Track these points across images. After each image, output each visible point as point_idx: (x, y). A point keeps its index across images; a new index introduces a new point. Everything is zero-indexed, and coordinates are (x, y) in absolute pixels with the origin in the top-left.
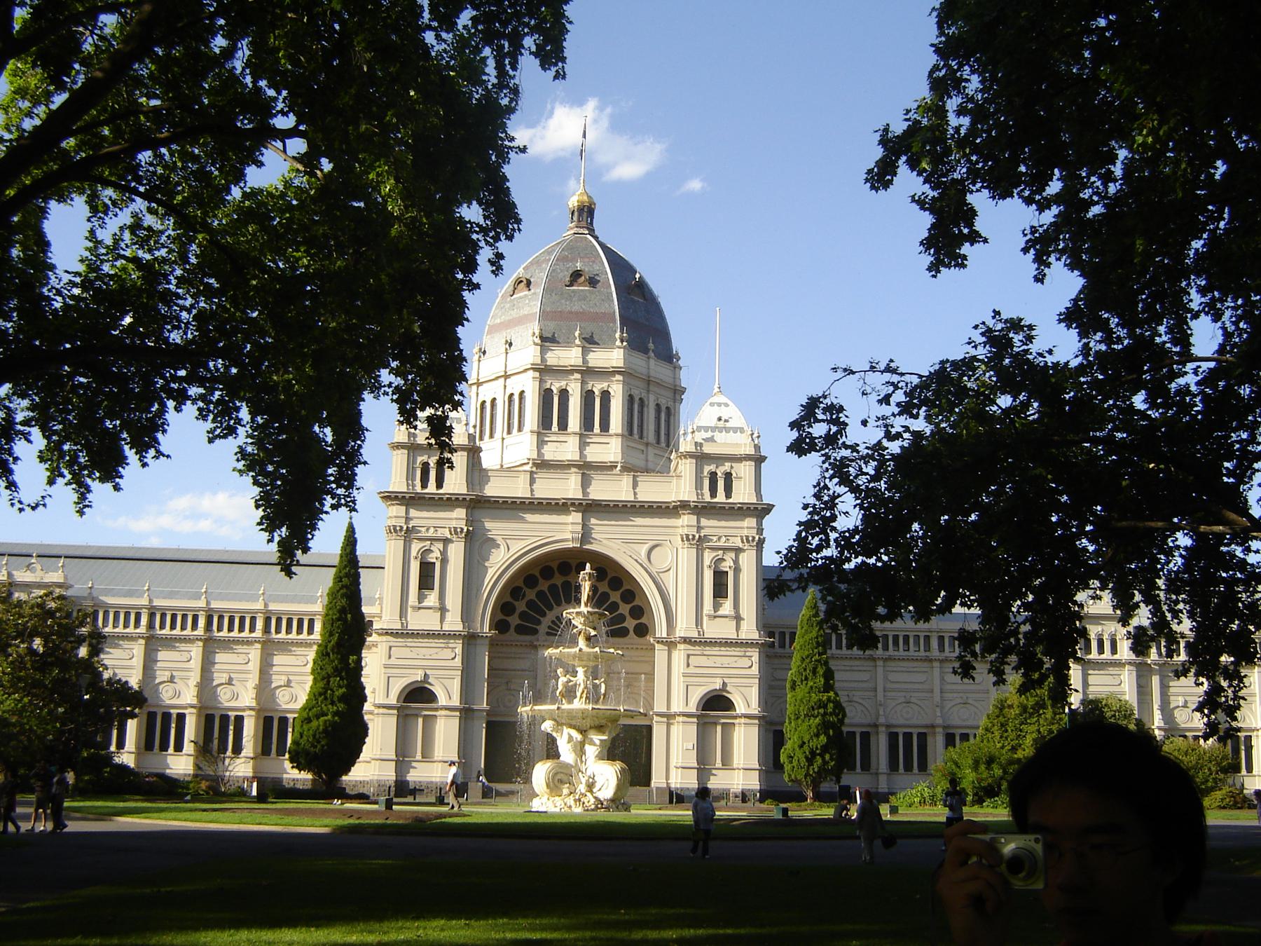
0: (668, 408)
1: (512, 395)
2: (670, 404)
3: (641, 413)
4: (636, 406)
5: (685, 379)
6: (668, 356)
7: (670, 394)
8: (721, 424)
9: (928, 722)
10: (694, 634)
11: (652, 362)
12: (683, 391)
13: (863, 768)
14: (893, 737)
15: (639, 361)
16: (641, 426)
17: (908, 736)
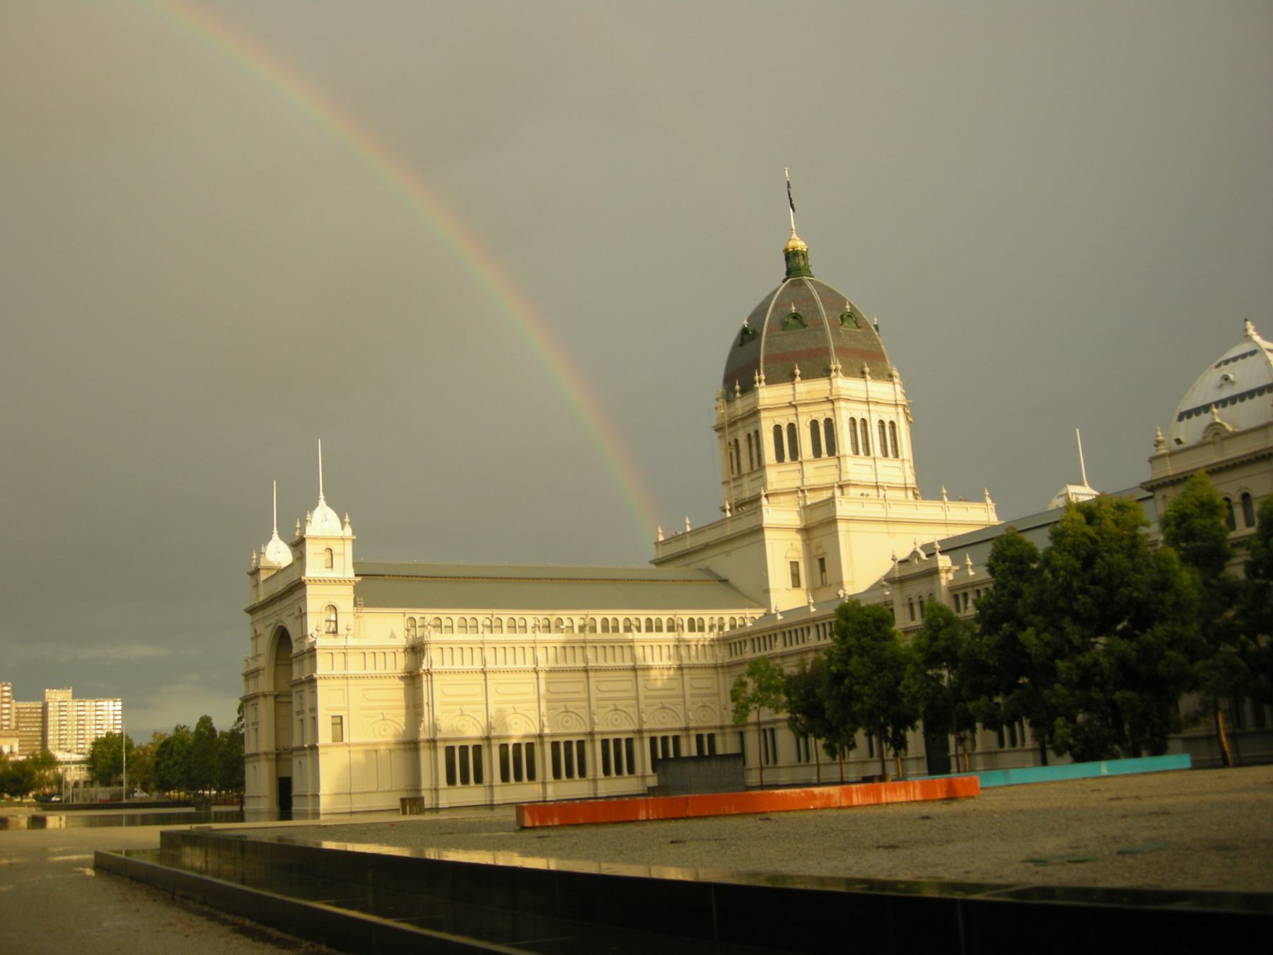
1: (749, 435)
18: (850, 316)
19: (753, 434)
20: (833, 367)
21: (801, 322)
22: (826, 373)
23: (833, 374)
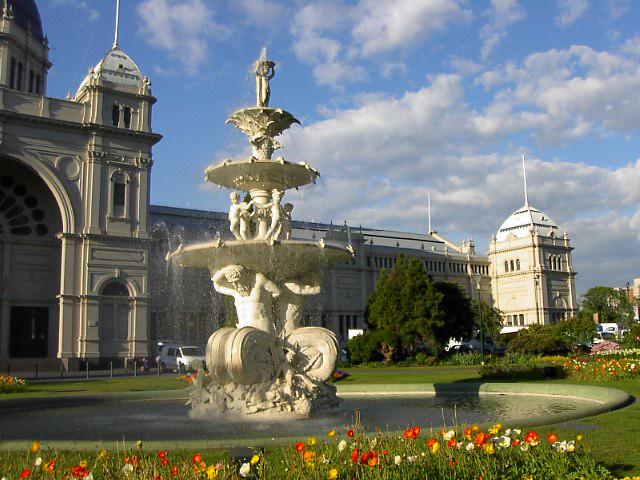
0: (38, 76)
2: (40, 73)
3: (20, 73)
4: (16, 68)
5: (51, 57)
6: (40, 39)
8: (121, 71)
10: (99, 233)
11: (30, 39)
12: (49, 65)
15: (20, 36)
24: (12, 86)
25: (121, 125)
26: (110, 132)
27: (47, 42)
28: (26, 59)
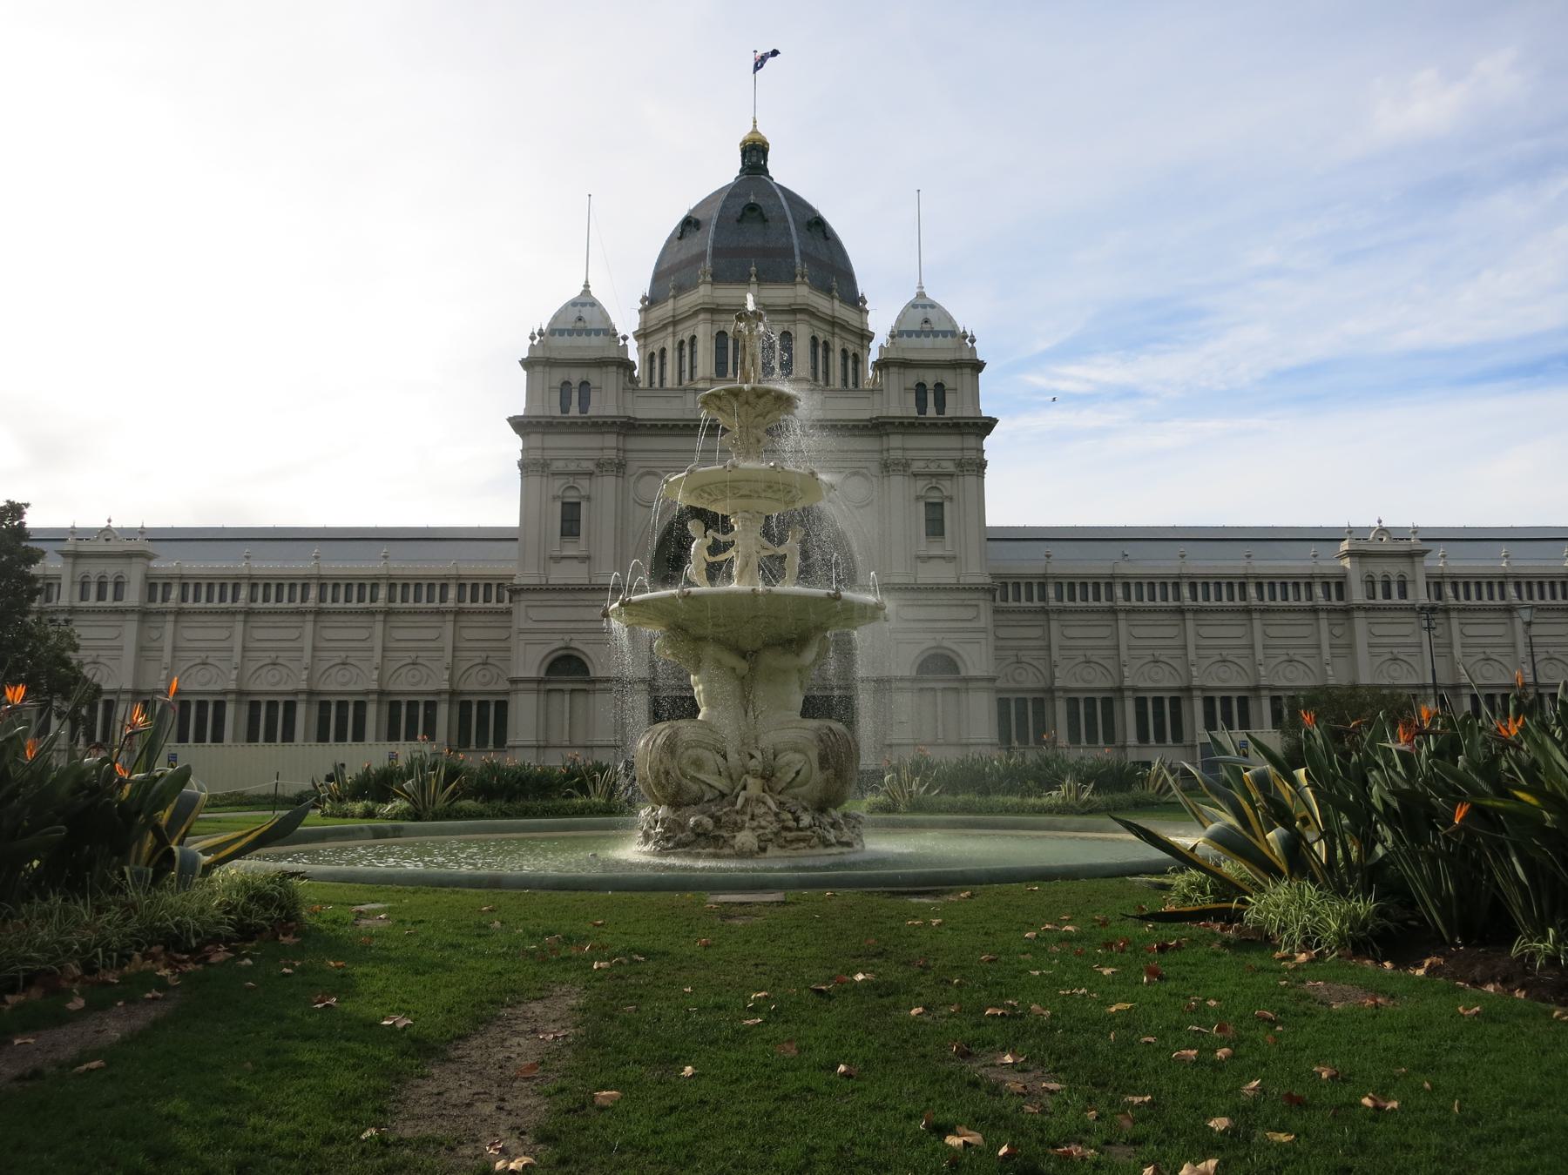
0: (855, 355)
1: (682, 342)
2: (858, 350)
3: (826, 358)
4: (820, 351)
6: (856, 302)
7: (858, 341)
9: (1184, 684)
11: (836, 302)
13: (1157, 741)
14: (1141, 703)
15: (821, 303)
16: (826, 373)
17: (1158, 702)
18: (817, 226)
19: (687, 341)
20: (798, 269)
21: (761, 214)
22: (791, 279)
23: (799, 279)
24: (816, 379)
25: (931, 412)
26: (912, 425)
27: (865, 302)
28: (833, 334)
